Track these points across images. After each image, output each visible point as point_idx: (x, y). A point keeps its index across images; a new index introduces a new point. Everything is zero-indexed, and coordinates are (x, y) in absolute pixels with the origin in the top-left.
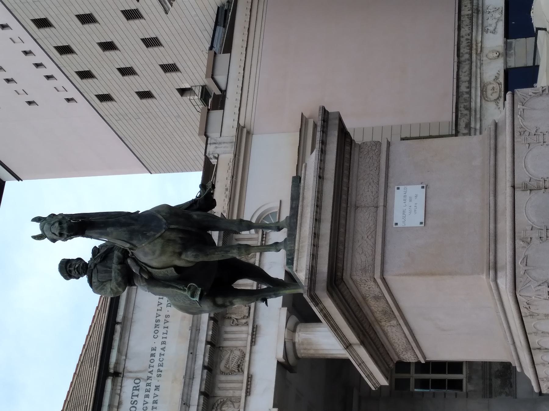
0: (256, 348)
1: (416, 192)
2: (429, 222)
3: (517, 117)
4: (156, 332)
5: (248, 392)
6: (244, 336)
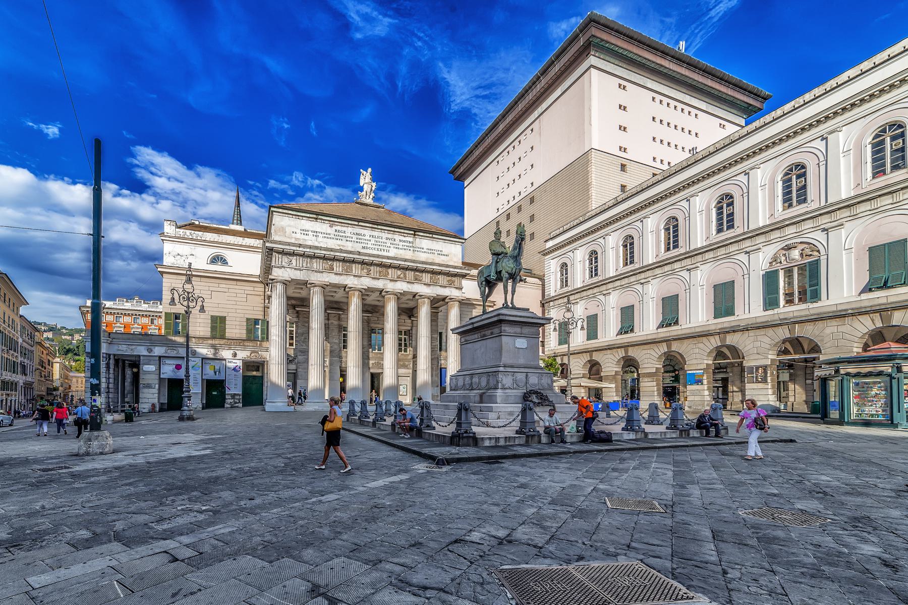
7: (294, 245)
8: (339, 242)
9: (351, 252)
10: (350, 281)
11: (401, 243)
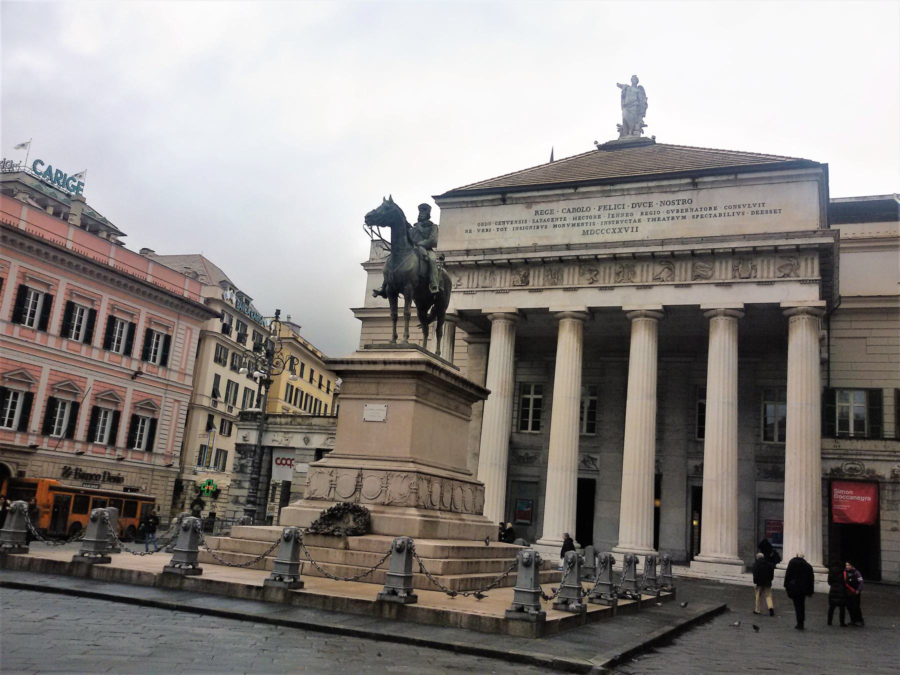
0: (713, 287)
1: (381, 416)
2: (366, 424)
3: (399, 473)
4: (730, 207)
5: (677, 286)
6: (723, 277)
7: (459, 253)
8: (541, 232)
9: (552, 248)
10: (555, 301)
11: (666, 208)
